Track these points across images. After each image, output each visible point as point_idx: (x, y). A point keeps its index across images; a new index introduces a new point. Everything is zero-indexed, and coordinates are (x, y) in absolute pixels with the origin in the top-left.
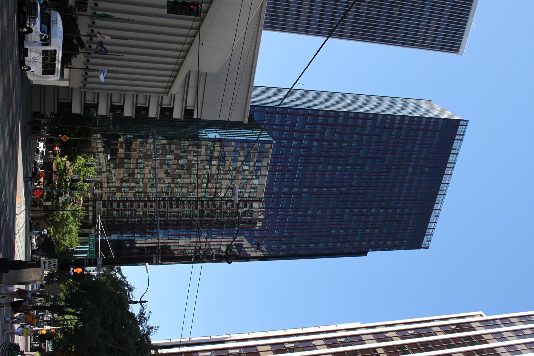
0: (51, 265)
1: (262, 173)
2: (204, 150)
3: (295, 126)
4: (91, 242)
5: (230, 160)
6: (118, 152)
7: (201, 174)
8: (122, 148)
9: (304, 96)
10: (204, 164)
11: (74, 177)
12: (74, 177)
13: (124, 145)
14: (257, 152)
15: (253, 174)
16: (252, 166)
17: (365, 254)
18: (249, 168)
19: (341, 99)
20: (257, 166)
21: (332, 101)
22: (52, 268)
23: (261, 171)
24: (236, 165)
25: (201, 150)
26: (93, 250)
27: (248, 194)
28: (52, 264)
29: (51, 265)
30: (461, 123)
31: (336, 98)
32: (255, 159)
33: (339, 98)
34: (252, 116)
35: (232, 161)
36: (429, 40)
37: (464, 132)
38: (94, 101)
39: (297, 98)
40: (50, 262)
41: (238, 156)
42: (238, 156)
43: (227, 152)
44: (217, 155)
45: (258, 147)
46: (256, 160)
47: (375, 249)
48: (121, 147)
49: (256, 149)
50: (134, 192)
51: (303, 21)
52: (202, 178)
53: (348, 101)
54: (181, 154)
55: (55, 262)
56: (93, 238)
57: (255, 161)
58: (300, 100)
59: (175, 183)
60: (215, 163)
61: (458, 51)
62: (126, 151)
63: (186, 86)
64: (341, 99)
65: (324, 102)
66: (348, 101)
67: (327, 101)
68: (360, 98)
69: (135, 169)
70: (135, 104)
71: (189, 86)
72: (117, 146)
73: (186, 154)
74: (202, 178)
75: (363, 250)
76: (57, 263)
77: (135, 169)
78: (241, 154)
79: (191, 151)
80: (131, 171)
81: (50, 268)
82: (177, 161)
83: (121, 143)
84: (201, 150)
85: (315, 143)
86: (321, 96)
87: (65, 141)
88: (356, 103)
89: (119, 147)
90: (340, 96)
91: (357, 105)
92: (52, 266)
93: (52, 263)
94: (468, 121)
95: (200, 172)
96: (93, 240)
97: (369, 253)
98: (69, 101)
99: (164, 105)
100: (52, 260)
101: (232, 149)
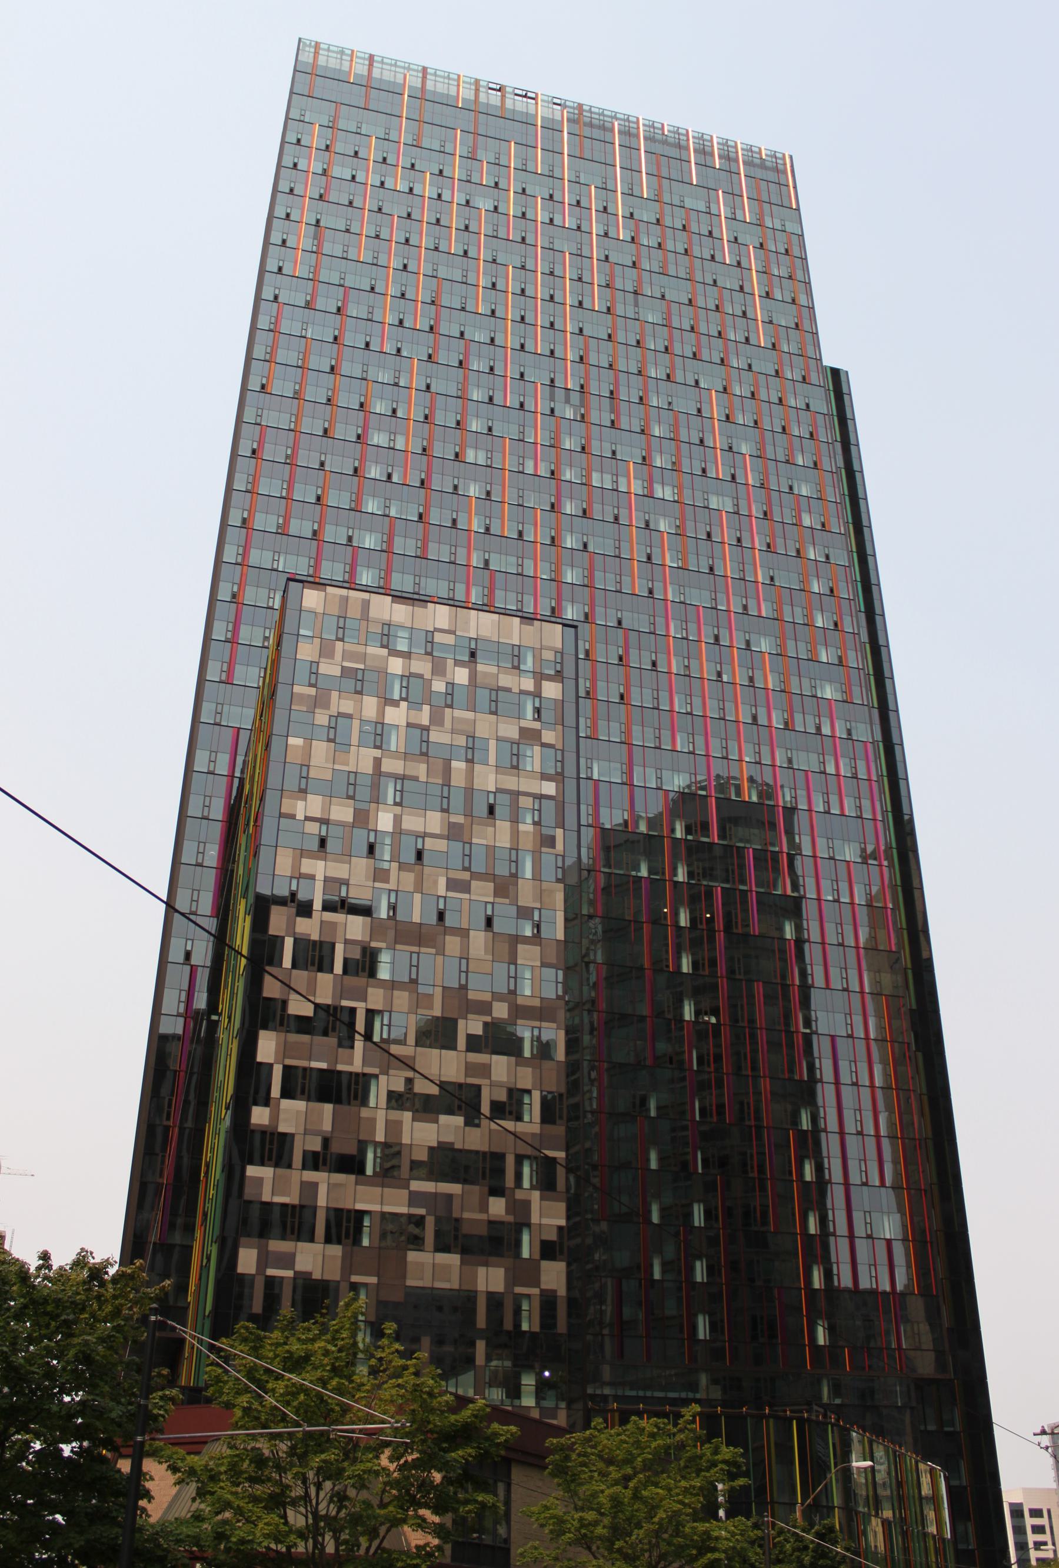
1: (445, 626)
5: (378, 753)
6: (317, 1275)
7: (442, 882)
8: (294, 1255)
10: (395, 865)
13: (276, 1245)
14: (339, 644)
15: (450, 663)
20: (410, 646)
23: (436, 630)
24: (403, 731)
25: (320, 877)
30: (307, 57)
32: (375, 651)
35: (380, 747)
37: (342, 52)
41: (356, 723)
42: (356, 723)
43: (337, 767)
45: (317, 641)
46: (382, 646)
48: (288, 1260)
49: (326, 651)
50: (536, 1195)
52: (466, 876)
57: (385, 651)
59: (490, 999)
60: (391, 816)
69: (410, 1192)
73: (339, 949)
74: (466, 876)
77: (410, 1192)
78: (347, 706)
80: (422, 1211)
82: (371, 990)
83: (264, 1260)
84: (320, 877)
85: (371, 506)
89: (289, 1273)
94: (300, 39)
95: (436, 883)
101: (321, 749)
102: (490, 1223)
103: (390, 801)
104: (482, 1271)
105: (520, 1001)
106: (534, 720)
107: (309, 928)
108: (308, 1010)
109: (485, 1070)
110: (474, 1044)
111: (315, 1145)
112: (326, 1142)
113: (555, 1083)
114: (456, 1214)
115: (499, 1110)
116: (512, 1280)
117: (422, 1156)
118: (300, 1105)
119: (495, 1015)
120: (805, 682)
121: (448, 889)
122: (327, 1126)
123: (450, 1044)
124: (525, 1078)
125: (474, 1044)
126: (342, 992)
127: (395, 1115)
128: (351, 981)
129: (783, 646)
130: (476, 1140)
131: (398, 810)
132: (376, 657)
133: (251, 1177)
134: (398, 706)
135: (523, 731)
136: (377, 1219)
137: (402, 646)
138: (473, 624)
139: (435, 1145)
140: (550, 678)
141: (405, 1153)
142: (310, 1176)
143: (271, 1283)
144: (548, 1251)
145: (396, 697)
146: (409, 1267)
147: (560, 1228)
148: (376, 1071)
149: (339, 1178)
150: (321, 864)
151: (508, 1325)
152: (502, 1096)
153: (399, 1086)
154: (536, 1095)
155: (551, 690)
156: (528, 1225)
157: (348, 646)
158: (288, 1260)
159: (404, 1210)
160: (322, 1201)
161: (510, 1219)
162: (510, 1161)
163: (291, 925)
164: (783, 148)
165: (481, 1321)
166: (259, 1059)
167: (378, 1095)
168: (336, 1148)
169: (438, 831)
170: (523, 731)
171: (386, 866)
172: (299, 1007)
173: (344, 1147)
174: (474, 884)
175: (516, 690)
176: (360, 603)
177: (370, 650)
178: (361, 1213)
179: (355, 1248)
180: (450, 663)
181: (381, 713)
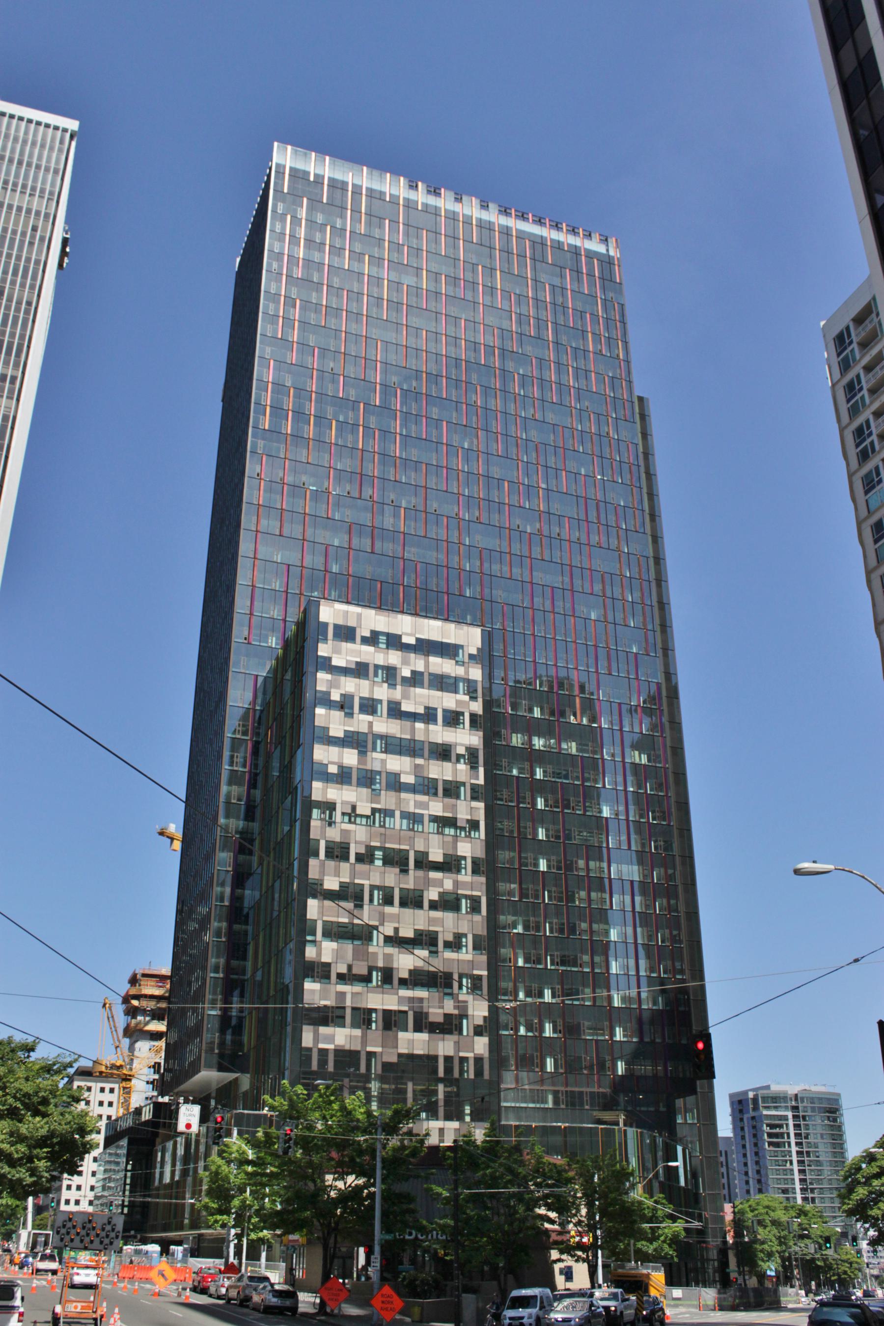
1: (409, 631)
6: (347, 1047)
8: (334, 1036)
13: (323, 1030)
44: (356, 757)
48: (331, 1039)
69: (399, 997)
72: (327, 1050)
77: (399, 997)
80: (405, 1008)
83: (316, 1039)
95: (408, 803)
102: (446, 1015)
104: (441, 1044)
106: (464, 694)
107: (334, 834)
108: (336, 887)
109: (441, 922)
110: (433, 906)
111: (343, 969)
112: (350, 967)
113: (482, 930)
114: (425, 1010)
115: (448, 945)
116: (458, 1046)
117: (405, 975)
118: (334, 945)
123: (418, 905)
124: (464, 927)
125: (433, 906)
126: (353, 874)
127: (389, 950)
128: (360, 867)
129: (605, 616)
130: (437, 965)
133: (308, 990)
134: (382, 686)
135: (458, 702)
136: (380, 1014)
138: (426, 629)
139: (412, 968)
141: (395, 973)
142: (341, 988)
143: (323, 1052)
144: (479, 1031)
146: (399, 1042)
147: (485, 1017)
148: (376, 923)
149: (358, 988)
151: (456, 1074)
152: (450, 938)
153: (390, 932)
154: (470, 937)
156: (467, 1016)
158: (331, 1039)
159: (394, 1007)
160: (348, 1003)
161: (456, 1012)
162: (456, 977)
163: (323, 833)
165: (441, 1073)
166: (308, 917)
167: (377, 938)
168: (355, 971)
169: (408, 770)
170: (458, 702)
172: (331, 884)
173: (361, 969)
176: (355, 615)
178: (371, 1011)
179: (369, 1031)
181: (372, 691)
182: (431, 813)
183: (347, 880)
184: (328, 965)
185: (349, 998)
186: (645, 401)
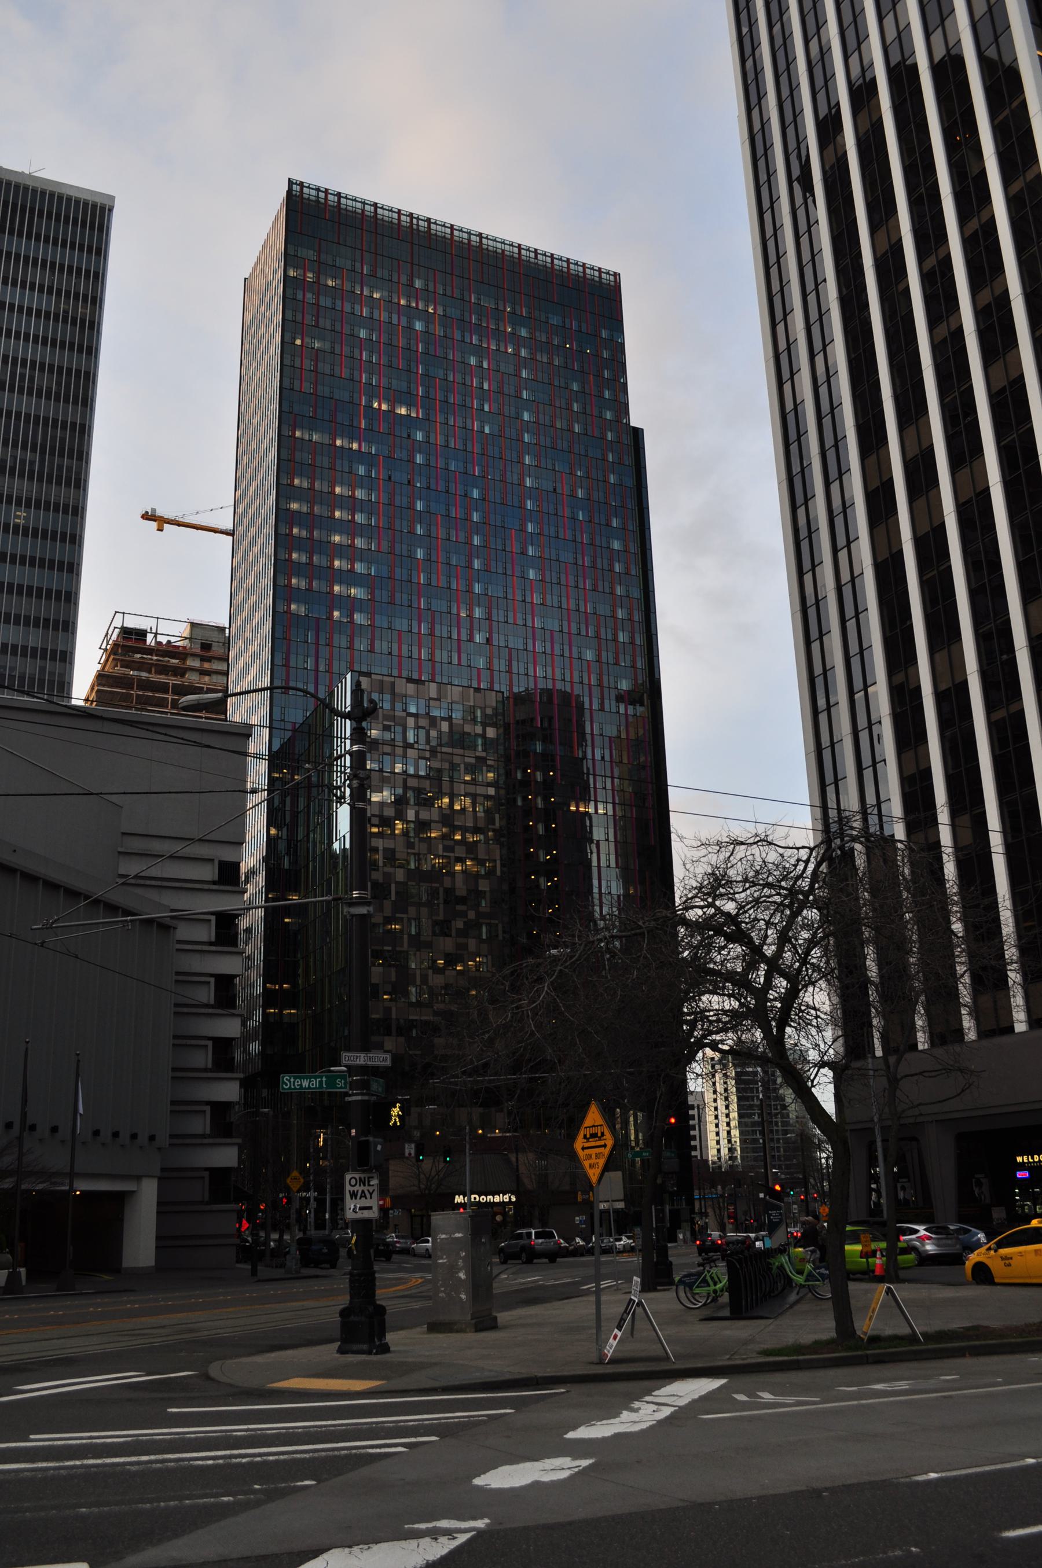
0: (363, 1192)
2: (381, 840)
3: (318, 619)
4: (301, 1085)
7: (441, 847)
8: (383, 1043)
9: (245, 600)
10: (417, 839)
11: (410, 1154)
12: (410, 1154)
16: (416, 723)
17: (637, 434)
18: (423, 728)
19: (248, 506)
20: (418, 709)
21: (253, 530)
22: (371, 1189)
25: (381, 848)
26: (324, 1079)
27: (488, 729)
28: (359, 1188)
29: (363, 1192)
31: (246, 521)
33: (246, 511)
34: (297, 726)
36: (78, 285)
38: (205, 1111)
39: (249, 619)
40: (354, 1195)
46: (403, 711)
47: (623, 409)
51: (43, 609)
52: (451, 843)
53: (252, 489)
54: (393, 898)
55: (353, 1182)
56: (292, 1080)
57: (404, 714)
58: (254, 608)
61: (103, 208)
62: (389, 1034)
63: (159, 883)
64: (248, 506)
65: (256, 549)
66: (252, 489)
67: (252, 543)
68: (246, 459)
70: (210, 1011)
71: (160, 876)
73: (393, 886)
75: (627, 440)
76: (357, 1176)
79: (384, 874)
81: (371, 1194)
82: (410, 908)
84: (381, 848)
86: (244, 558)
87: (302, 1180)
88: (257, 470)
90: (240, 510)
91: (260, 465)
92: (366, 1188)
93: (355, 1189)
96: (295, 1078)
97: (633, 424)
98: (206, 1174)
99: (210, 937)
100: (348, 1188)
103: (412, 802)
105: (481, 909)
106: (483, 751)
119: (469, 917)
120: (612, 679)
121: (443, 852)
122: (393, 979)
129: (599, 656)
131: (416, 808)
132: (401, 717)
135: (477, 758)
137: (413, 710)
140: (491, 726)
145: (412, 741)
150: (381, 840)
155: (491, 732)
157: (385, 712)
160: (394, 1016)
164: (613, 269)
171: (412, 840)
174: (457, 847)
175: (473, 734)
177: (397, 713)
180: (439, 718)
182: (457, 855)
183: (390, 915)
184: (378, 985)
185: (394, 1010)
186: (640, 431)
